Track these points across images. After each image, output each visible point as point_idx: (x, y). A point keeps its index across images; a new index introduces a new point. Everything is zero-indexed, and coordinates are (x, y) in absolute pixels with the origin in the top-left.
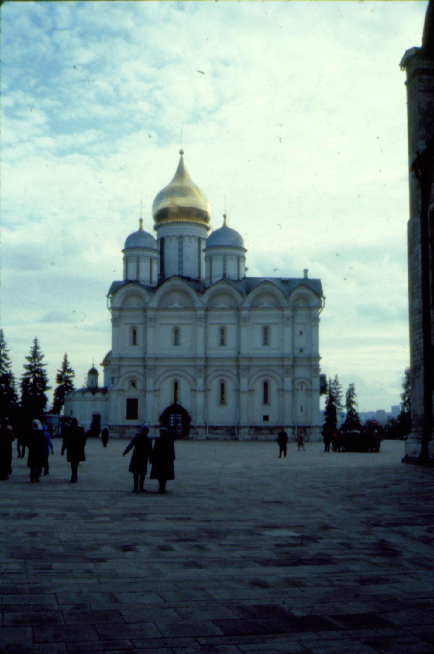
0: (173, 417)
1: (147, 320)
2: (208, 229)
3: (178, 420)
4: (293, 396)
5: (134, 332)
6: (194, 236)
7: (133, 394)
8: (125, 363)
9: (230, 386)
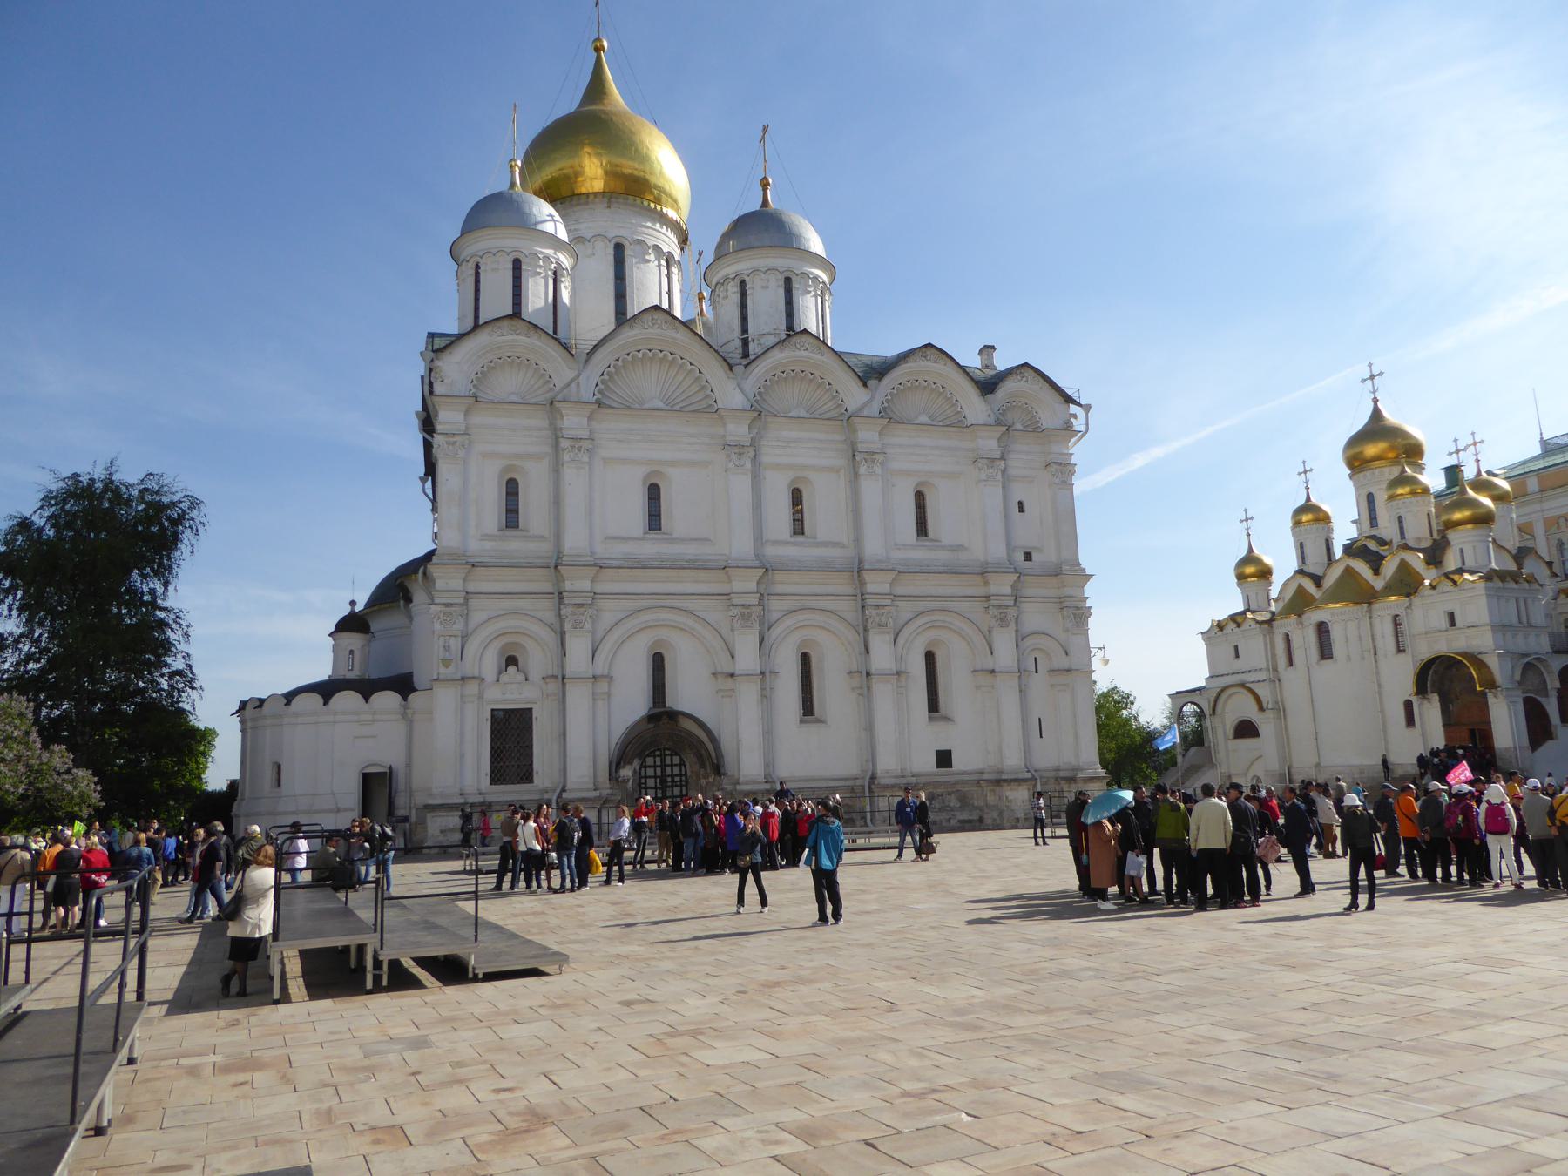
0: (655, 767)
1: (564, 444)
3: (672, 776)
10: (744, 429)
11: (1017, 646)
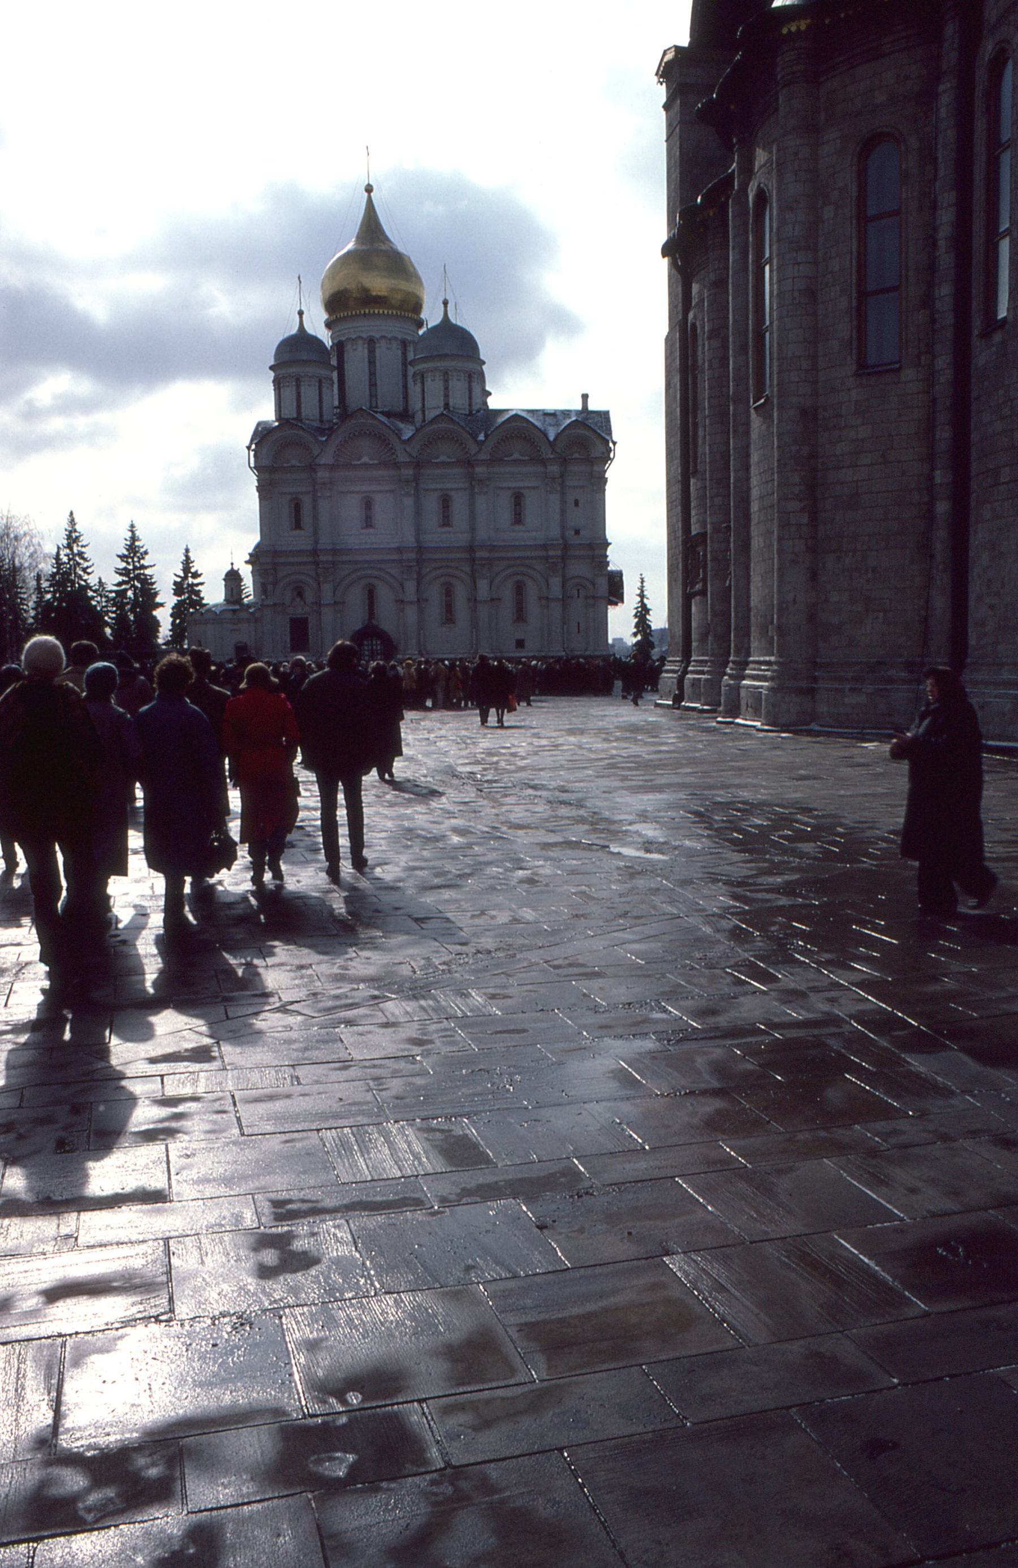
2: (420, 324)
4: (565, 607)
5: (297, 508)
6: (395, 338)
7: (299, 611)
8: (282, 560)
9: (461, 595)
10: (411, 472)
11: (563, 587)
